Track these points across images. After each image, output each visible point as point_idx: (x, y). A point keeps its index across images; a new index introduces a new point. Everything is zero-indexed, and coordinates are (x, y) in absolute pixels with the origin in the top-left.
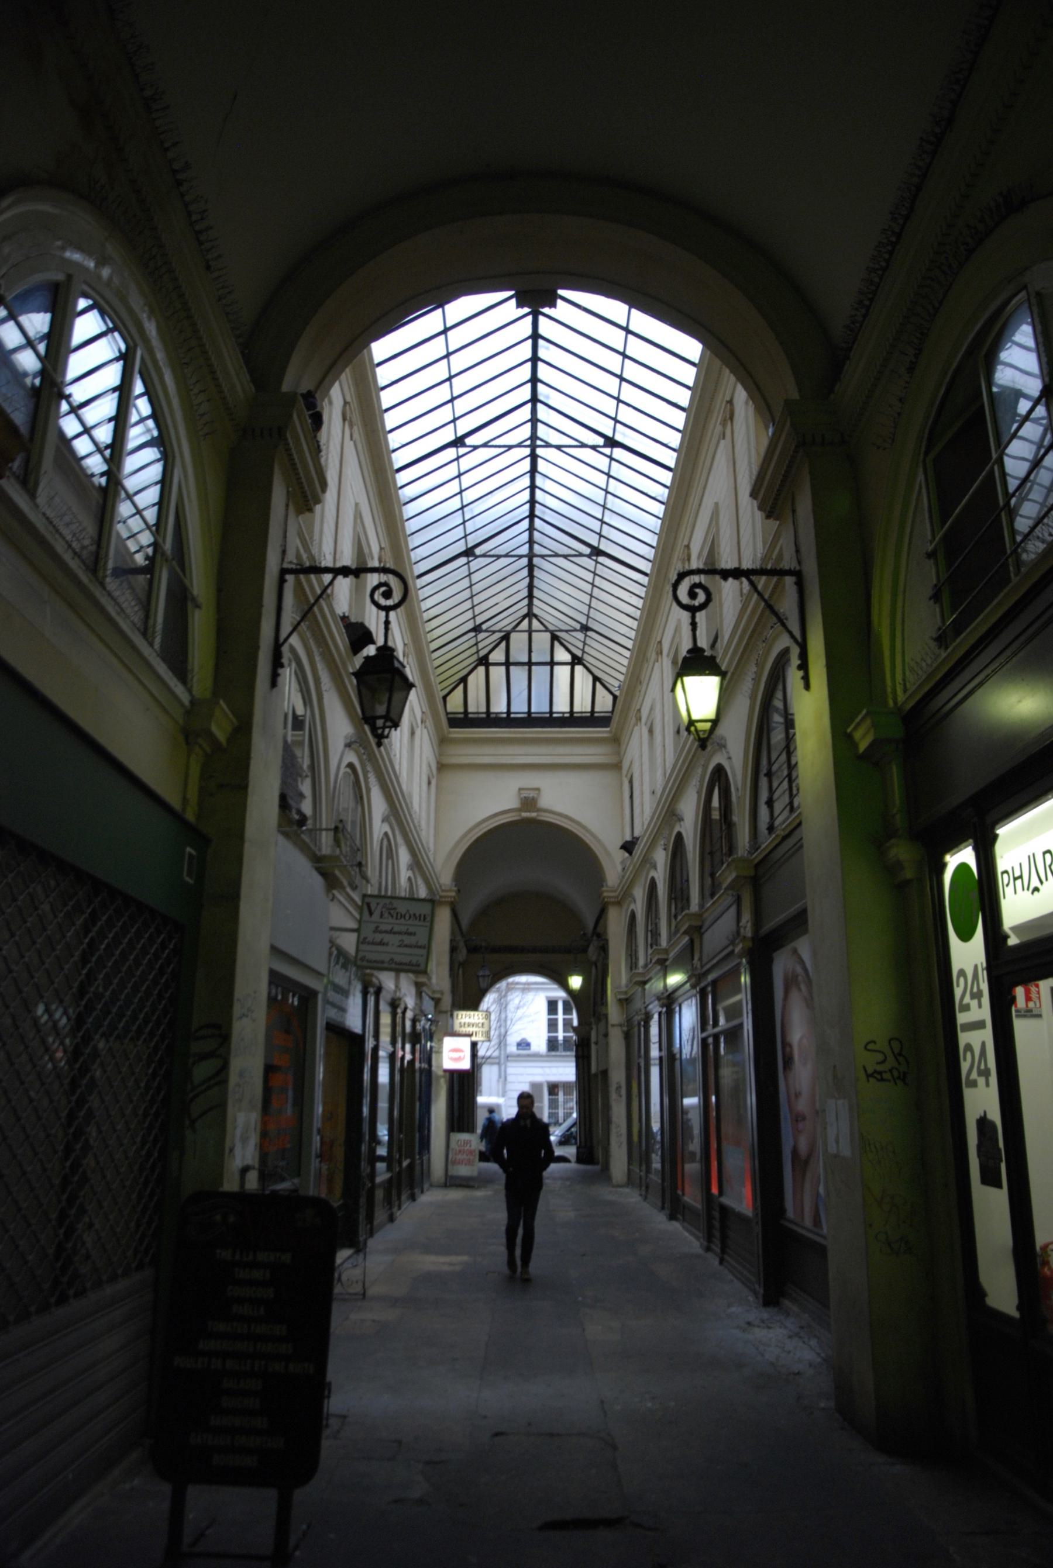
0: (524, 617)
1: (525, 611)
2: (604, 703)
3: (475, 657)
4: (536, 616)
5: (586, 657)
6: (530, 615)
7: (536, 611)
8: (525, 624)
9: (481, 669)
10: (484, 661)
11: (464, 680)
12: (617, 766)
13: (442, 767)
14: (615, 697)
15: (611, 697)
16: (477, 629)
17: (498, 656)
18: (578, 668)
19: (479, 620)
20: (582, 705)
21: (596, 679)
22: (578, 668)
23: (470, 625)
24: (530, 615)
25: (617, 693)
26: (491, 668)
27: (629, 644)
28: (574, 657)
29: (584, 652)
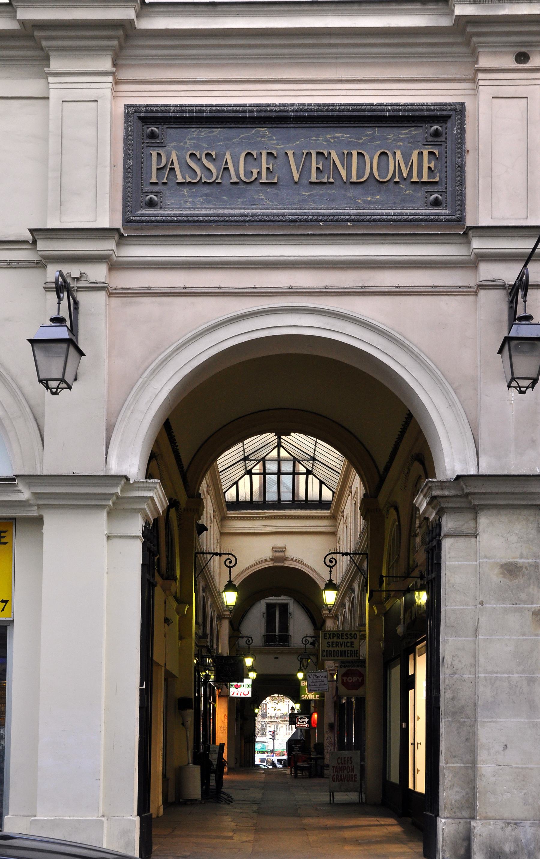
0: (275, 448)
1: (276, 444)
2: (327, 495)
3: (243, 472)
4: (283, 447)
5: (314, 471)
6: (279, 446)
7: (282, 444)
8: (274, 453)
9: (247, 477)
10: (249, 473)
11: (236, 483)
12: (334, 534)
13: (222, 534)
14: (333, 492)
15: (332, 493)
16: (245, 459)
17: (258, 469)
18: (310, 476)
19: (246, 455)
20: (314, 494)
21: (321, 483)
22: (310, 476)
23: (243, 457)
24: (279, 446)
25: (334, 490)
26: (253, 476)
27: (340, 471)
28: (307, 469)
29: (312, 468)
